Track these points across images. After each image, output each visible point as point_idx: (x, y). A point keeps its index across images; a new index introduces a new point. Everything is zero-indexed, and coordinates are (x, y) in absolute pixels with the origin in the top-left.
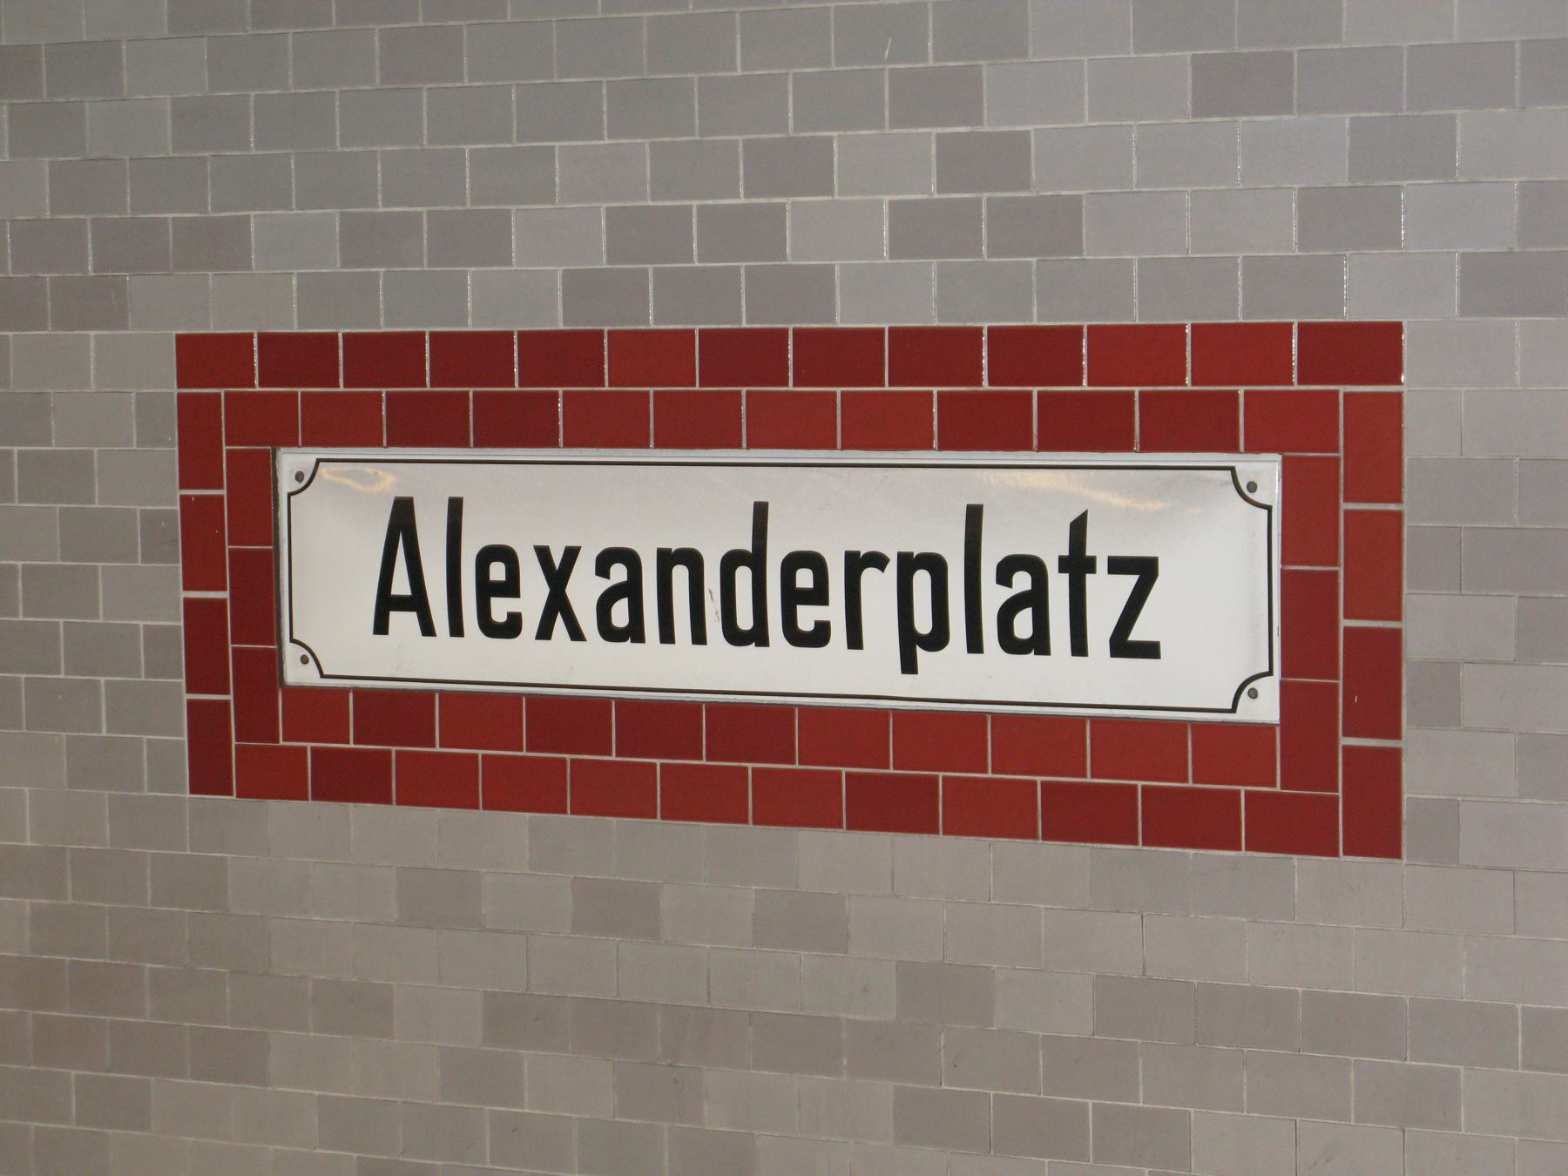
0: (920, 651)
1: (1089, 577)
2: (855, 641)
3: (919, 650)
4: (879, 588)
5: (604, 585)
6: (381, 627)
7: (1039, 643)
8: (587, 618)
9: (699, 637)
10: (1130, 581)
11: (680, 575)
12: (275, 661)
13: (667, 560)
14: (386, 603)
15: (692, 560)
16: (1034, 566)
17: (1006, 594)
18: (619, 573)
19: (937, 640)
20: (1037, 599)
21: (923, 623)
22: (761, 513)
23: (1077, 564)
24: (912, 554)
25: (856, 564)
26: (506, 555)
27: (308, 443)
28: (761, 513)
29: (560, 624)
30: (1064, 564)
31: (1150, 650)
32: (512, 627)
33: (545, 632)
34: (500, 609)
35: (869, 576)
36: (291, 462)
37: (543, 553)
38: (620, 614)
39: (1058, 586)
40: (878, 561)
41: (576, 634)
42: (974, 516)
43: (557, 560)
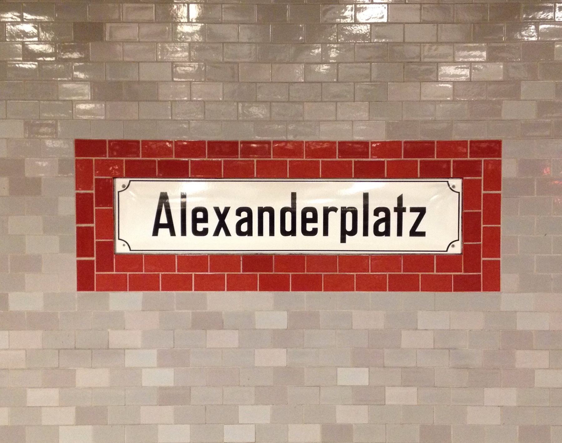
0: (347, 236)
1: (404, 213)
2: (326, 233)
3: (347, 236)
4: (335, 219)
5: (239, 218)
6: (155, 233)
7: (387, 233)
8: (232, 228)
9: (272, 233)
10: (418, 214)
11: (266, 215)
12: (112, 245)
13: (261, 211)
14: (158, 226)
15: (271, 211)
16: (386, 211)
17: (377, 218)
18: (244, 215)
19: (354, 232)
20: (387, 220)
21: (349, 228)
22: (294, 196)
23: (400, 210)
24: (262, 207)
25: (326, 211)
26: (204, 211)
27: (127, 176)
28: (294, 196)
29: (222, 231)
30: (396, 210)
31: (423, 234)
32: (205, 232)
33: (217, 233)
34: (200, 227)
35: (331, 214)
36: (119, 183)
37: (217, 210)
38: (244, 227)
39: (394, 217)
40: (335, 209)
41: (228, 233)
42: (366, 196)
43: (222, 212)
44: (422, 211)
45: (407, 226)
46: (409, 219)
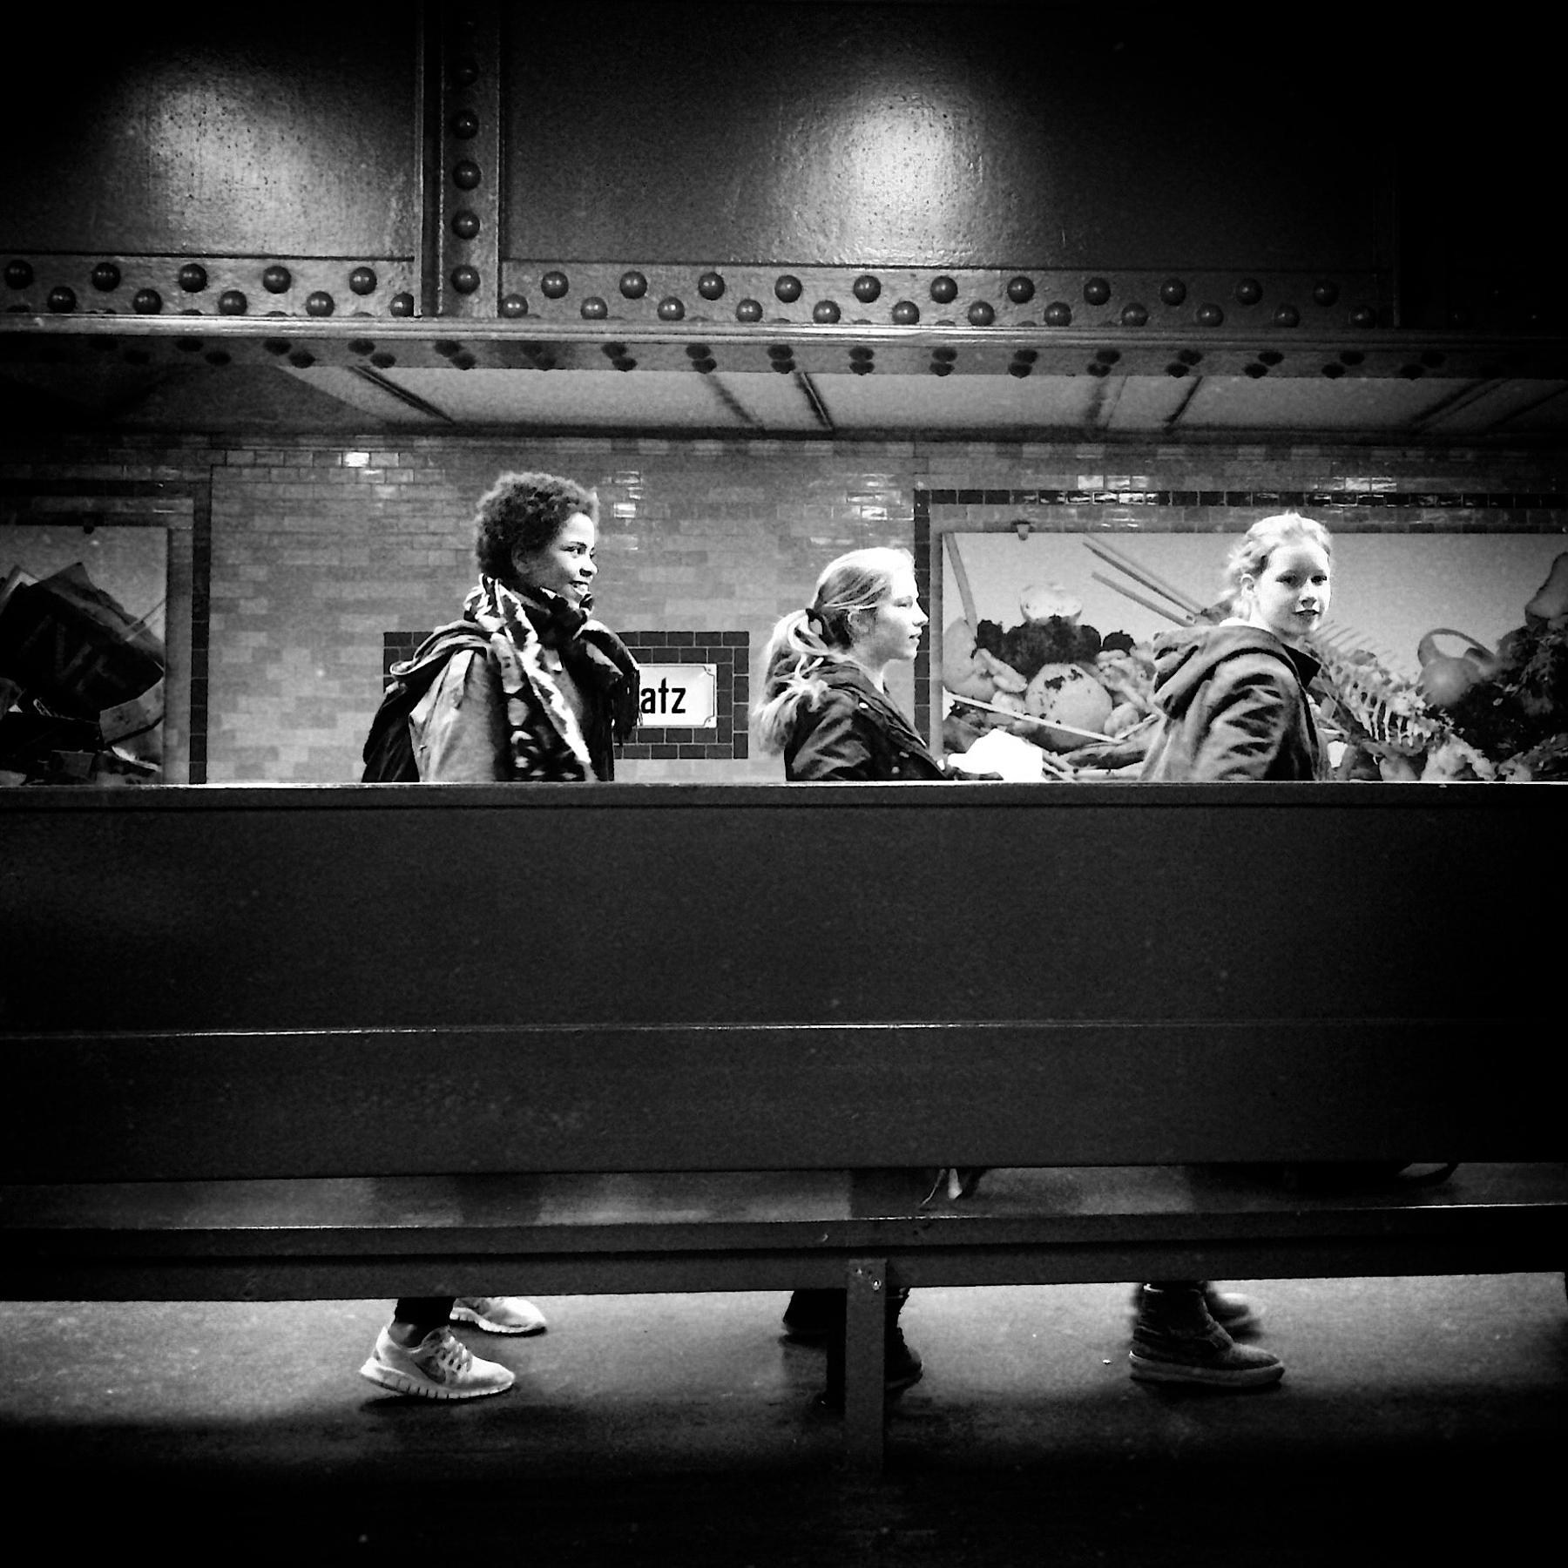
7: (653, 710)
16: (652, 691)
20: (652, 699)
23: (664, 690)
30: (660, 690)
31: (683, 711)
39: (658, 696)
44: (682, 691)
45: (670, 705)
46: (671, 698)
